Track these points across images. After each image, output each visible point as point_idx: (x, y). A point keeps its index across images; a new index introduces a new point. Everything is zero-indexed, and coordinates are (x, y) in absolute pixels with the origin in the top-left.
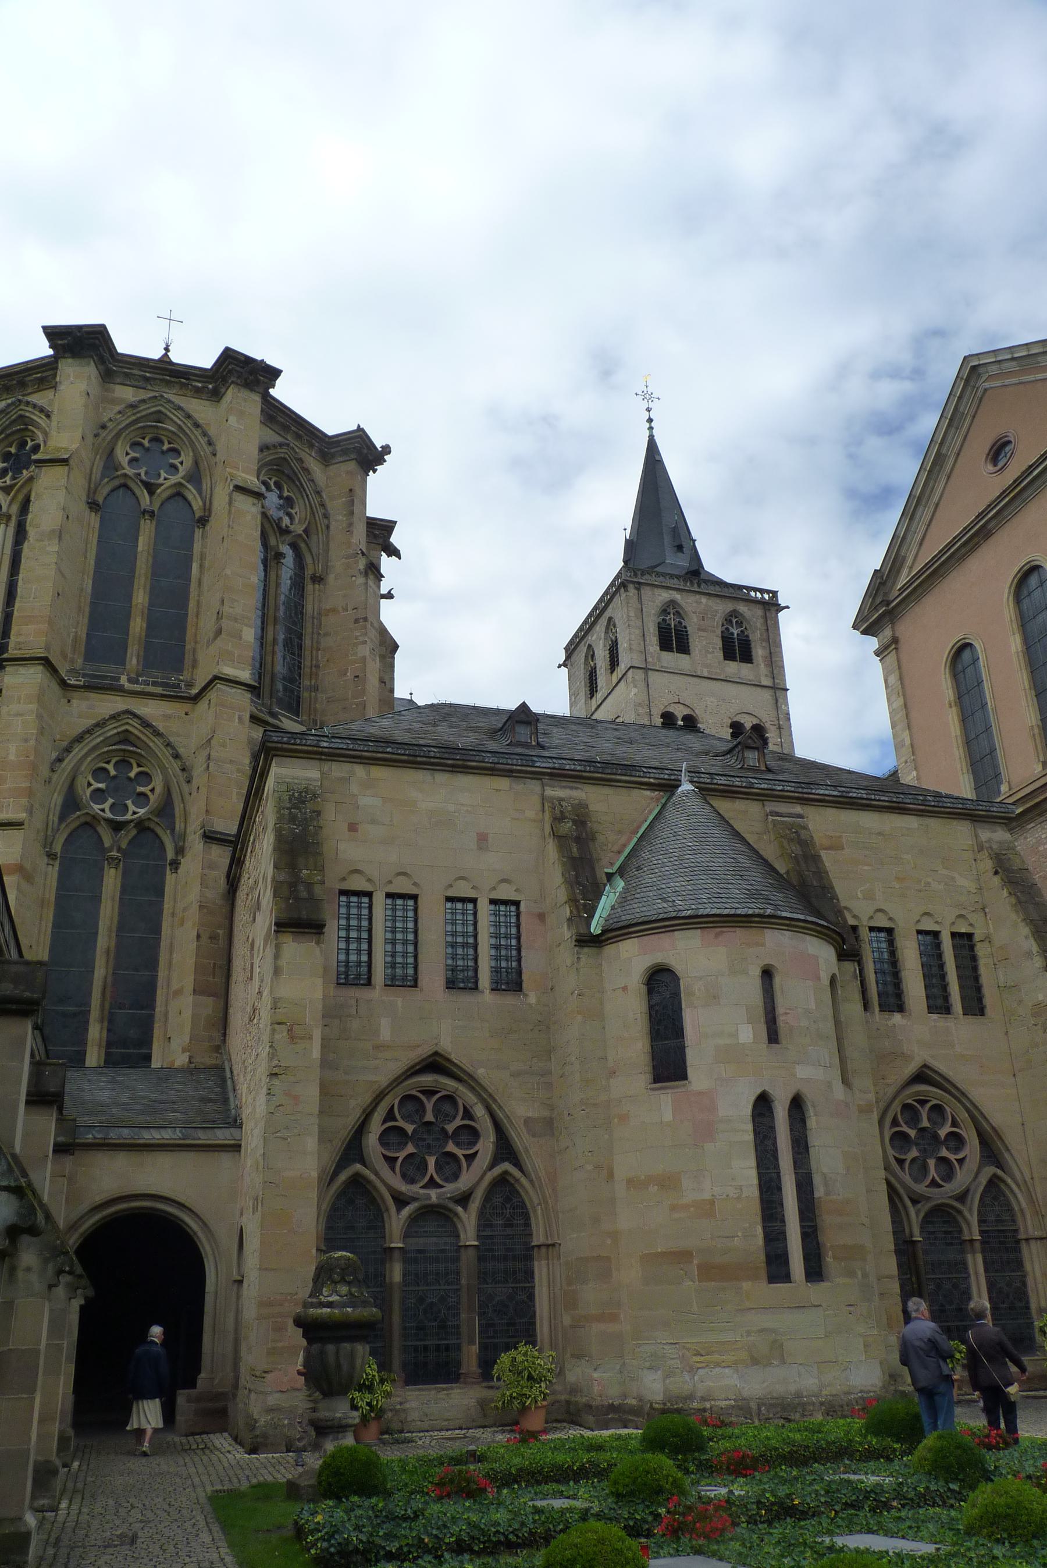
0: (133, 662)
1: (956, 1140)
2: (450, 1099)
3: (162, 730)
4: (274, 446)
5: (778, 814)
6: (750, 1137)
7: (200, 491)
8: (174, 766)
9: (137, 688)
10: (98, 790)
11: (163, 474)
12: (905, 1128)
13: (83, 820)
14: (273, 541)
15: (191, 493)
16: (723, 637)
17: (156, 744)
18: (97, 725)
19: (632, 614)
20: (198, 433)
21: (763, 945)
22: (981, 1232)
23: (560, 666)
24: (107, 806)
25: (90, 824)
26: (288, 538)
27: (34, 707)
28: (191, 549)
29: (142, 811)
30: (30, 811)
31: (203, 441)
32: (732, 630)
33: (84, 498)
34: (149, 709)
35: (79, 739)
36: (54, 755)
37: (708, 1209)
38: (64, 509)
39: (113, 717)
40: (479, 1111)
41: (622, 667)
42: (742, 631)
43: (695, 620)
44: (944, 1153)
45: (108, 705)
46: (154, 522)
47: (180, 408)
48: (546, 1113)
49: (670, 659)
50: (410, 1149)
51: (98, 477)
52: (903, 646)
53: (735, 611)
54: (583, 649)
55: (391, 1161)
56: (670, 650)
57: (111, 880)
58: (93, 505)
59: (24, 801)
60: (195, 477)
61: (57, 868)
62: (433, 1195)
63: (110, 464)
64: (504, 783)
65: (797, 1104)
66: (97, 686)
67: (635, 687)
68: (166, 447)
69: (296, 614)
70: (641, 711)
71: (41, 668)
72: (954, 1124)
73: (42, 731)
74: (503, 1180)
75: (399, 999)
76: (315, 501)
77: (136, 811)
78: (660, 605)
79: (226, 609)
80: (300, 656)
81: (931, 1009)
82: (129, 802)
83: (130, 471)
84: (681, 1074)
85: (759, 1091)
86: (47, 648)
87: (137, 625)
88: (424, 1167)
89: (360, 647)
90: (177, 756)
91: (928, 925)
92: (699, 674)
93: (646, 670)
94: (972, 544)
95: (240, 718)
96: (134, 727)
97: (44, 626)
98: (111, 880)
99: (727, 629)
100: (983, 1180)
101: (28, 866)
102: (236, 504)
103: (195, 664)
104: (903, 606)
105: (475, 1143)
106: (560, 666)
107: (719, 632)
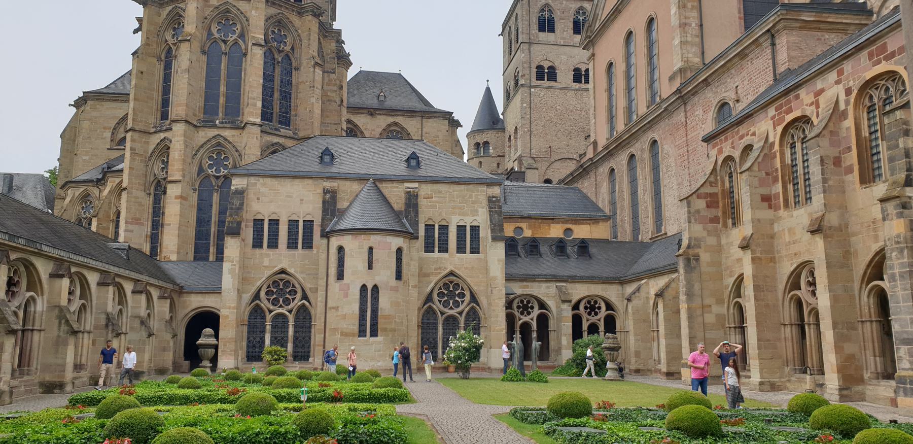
1: (462, 295)
2: (288, 282)
3: (231, 141)
4: (275, 15)
5: (408, 188)
6: (358, 297)
7: (244, 42)
8: (237, 154)
9: (222, 125)
10: (210, 164)
11: (230, 35)
12: (444, 291)
13: (205, 176)
14: (276, 56)
15: (241, 42)
16: (574, 22)
17: (229, 146)
18: (208, 141)
19: (524, 13)
20: (242, 16)
21: (369, 240)
22: (465, 324)
23: (499, 35)
24: (213, 170)
25: (208, 176)
26: (282, 54)
27: (183, 138)
28: (242, 66)
29: (226, 171)
30: (184, 176)
31: (244, 19)
32: (579, 17)
33: (199, 50)
34: (227, 133)
35: (202, 146)
36: (193, 153)
37: (344, 317)
38: (189, 60)
39: (213, 137)
40: (297, 285)
41: (519, 42)
42: (585, 18)
43: (559, 14)
44: (457, 298)
45: (212, 132)
46: (227, 57)
47: (235, 6)
48: (316, 286)
49: (543, 36)
50: (275, 296)
51: (205, 39)
52: (596, 58)
53: (581, 6)
54: (508, 27)
55: (269, 300)
56: (544, 31)
57: (216, 197)
58: (204, 52)
59: (181, 173)
60: (242, 36)
61: (197, 193)
62: (280, 310)
63: (210, 34)
64: (310, 181)
65: (375, 288)
66: (208, 124)
67: (523, 53)
68: (231, 22)
70: (525, 65)
71: (184, 124)
72: (462, 289)
73: (186, 146)
74: (303, 305)
75: (271, 252)
76: (295, 34)
77: (223, 172)
78: (540, 7)
79: (250, 95)
80: (290, 102)
81: (458, 252)
82: (221, 168)
83: (217, 36)
84: (343, 279)
85: (362, 284)
86: (186, 115)
87: (222, 100)
88: (279, 301)
89: (312, 98)
90: (237, 151)
91: (462, 223)
92: (558, 43)
93: (530, 43)
94: (615, 15)
95: (257, 137)
96: (222, 141)
97: (185, 107)
98: (216, 197)
99: (577, 17)
100: (468, 308)
101: (184, 195)
102: (253, 51)
103: (243, 115)
104: (596, 38)
105: (295, 295)
106: (499, 35)
107: (572, 20)
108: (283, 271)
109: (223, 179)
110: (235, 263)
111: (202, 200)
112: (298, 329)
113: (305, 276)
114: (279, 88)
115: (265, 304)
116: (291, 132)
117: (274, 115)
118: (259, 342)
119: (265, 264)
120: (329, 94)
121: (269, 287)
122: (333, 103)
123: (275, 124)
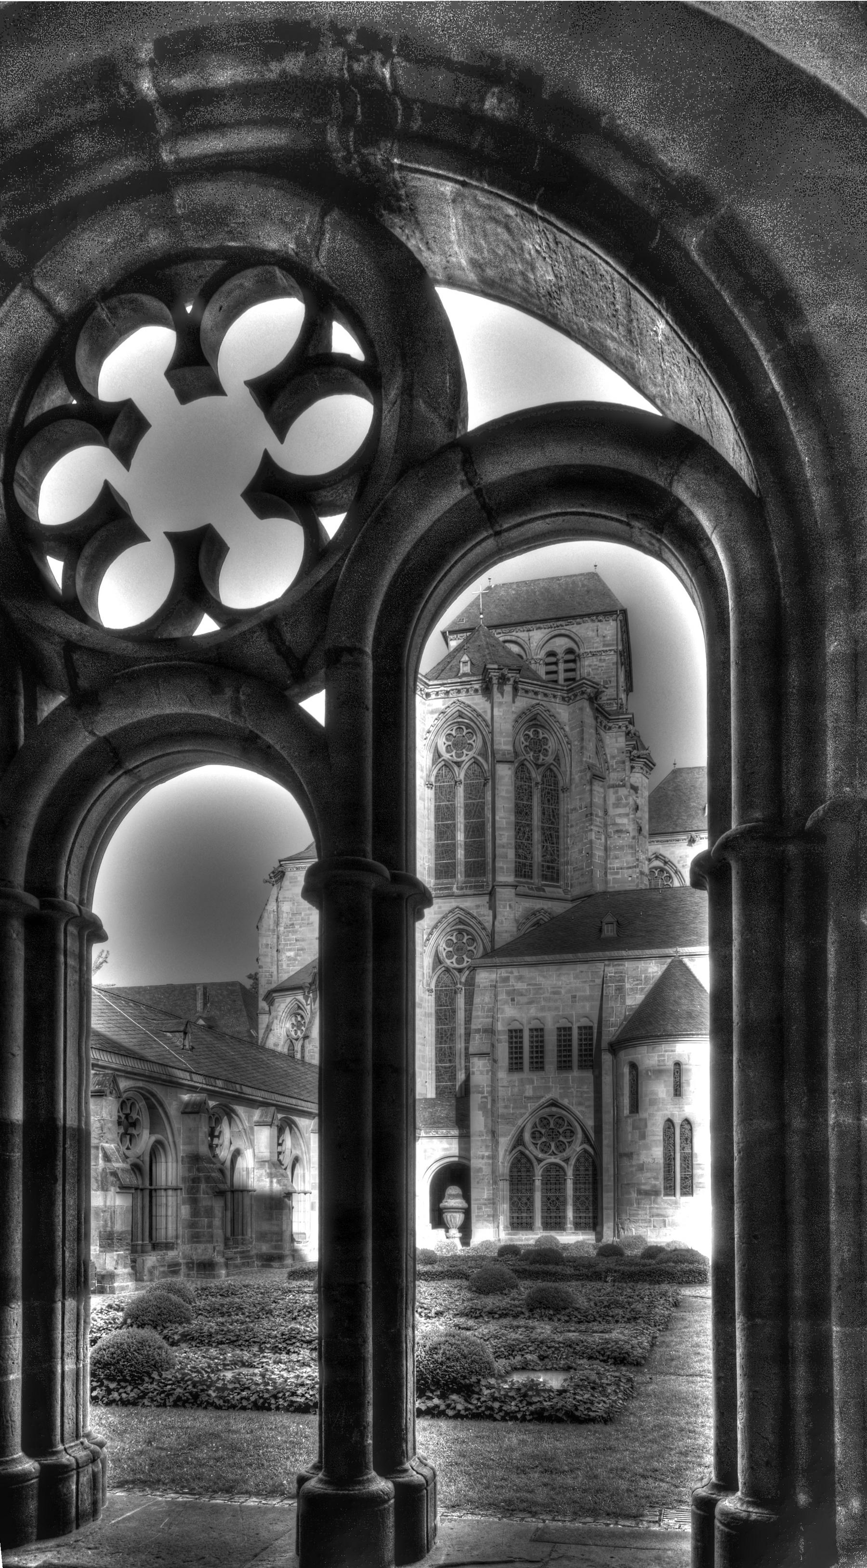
0: (460, 877)
3: (475, 914)
50: (544, 1139)
55: (535, 1144)
62: (553, 1160)
69: (554, 816)
80: (557, 843)
88: (549, 1147)
108: (554, 1104)
109: (467, 972)
110: (486, 1094)
111: (441, 1006)
112: (578, 1186)
113: (584, 1109)
114: (540, 824)
115: (534, 1151)
116: (560, 891)
117: (535, 868)
118: (526, 1204)
119: (527, 1094)
120: (619, 821)
121: (535, 1126)
122: (623, 835)
123: (537, 880)
